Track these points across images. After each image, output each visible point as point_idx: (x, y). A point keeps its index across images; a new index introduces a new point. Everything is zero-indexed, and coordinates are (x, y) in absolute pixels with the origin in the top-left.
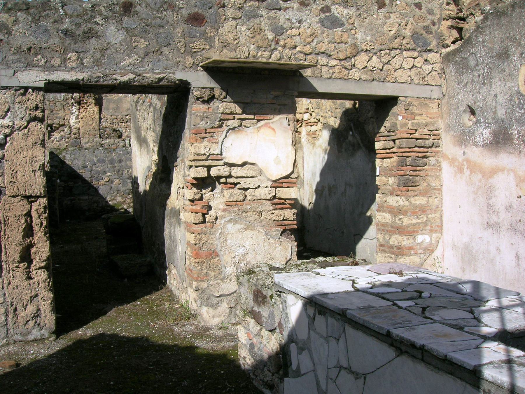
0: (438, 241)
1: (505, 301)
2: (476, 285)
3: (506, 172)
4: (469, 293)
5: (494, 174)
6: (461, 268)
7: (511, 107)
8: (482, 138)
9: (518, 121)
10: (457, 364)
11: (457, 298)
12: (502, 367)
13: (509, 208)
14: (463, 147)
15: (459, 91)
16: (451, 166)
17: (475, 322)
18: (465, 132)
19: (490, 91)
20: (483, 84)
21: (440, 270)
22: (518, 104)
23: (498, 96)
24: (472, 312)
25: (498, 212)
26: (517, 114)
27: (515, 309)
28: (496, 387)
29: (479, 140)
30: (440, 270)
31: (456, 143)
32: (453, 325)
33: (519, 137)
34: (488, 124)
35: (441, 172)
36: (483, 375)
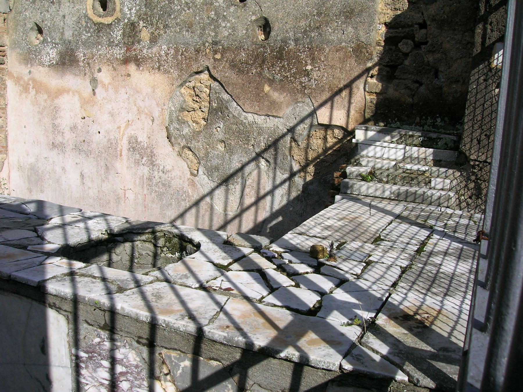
0: (3, 162)
1: (68, 218)
2: (40, 204)
3: (71, 93)
4: (33, 212)
5: (60, 95)
6: (28, 189)
7: (78, 29)
8: (48, 57)
9: (84, 44)
10: (21, 283)
11: (20, 218)
12: (65, 280)
13: (74, 128)
14: (29, 66)
15: (26, 7)
16: (16, 84)
17: (39, 240)
18: (31, 51)
19: (58, 11)
20: (51, 2)
21: (6, 192)
22: (85, 27)
23: (66, 18)
24: (35, 231)
25: (63, 133)
26: (84, 37)
27: (77, 225)
28: (60, 299)
29: (46, 59)
30: (6, 192)
31: (22, 61)
32: (16, 245)
33: (84, 60)
34: (55, 44)
35: (5, 91)
36: (47, 290)
